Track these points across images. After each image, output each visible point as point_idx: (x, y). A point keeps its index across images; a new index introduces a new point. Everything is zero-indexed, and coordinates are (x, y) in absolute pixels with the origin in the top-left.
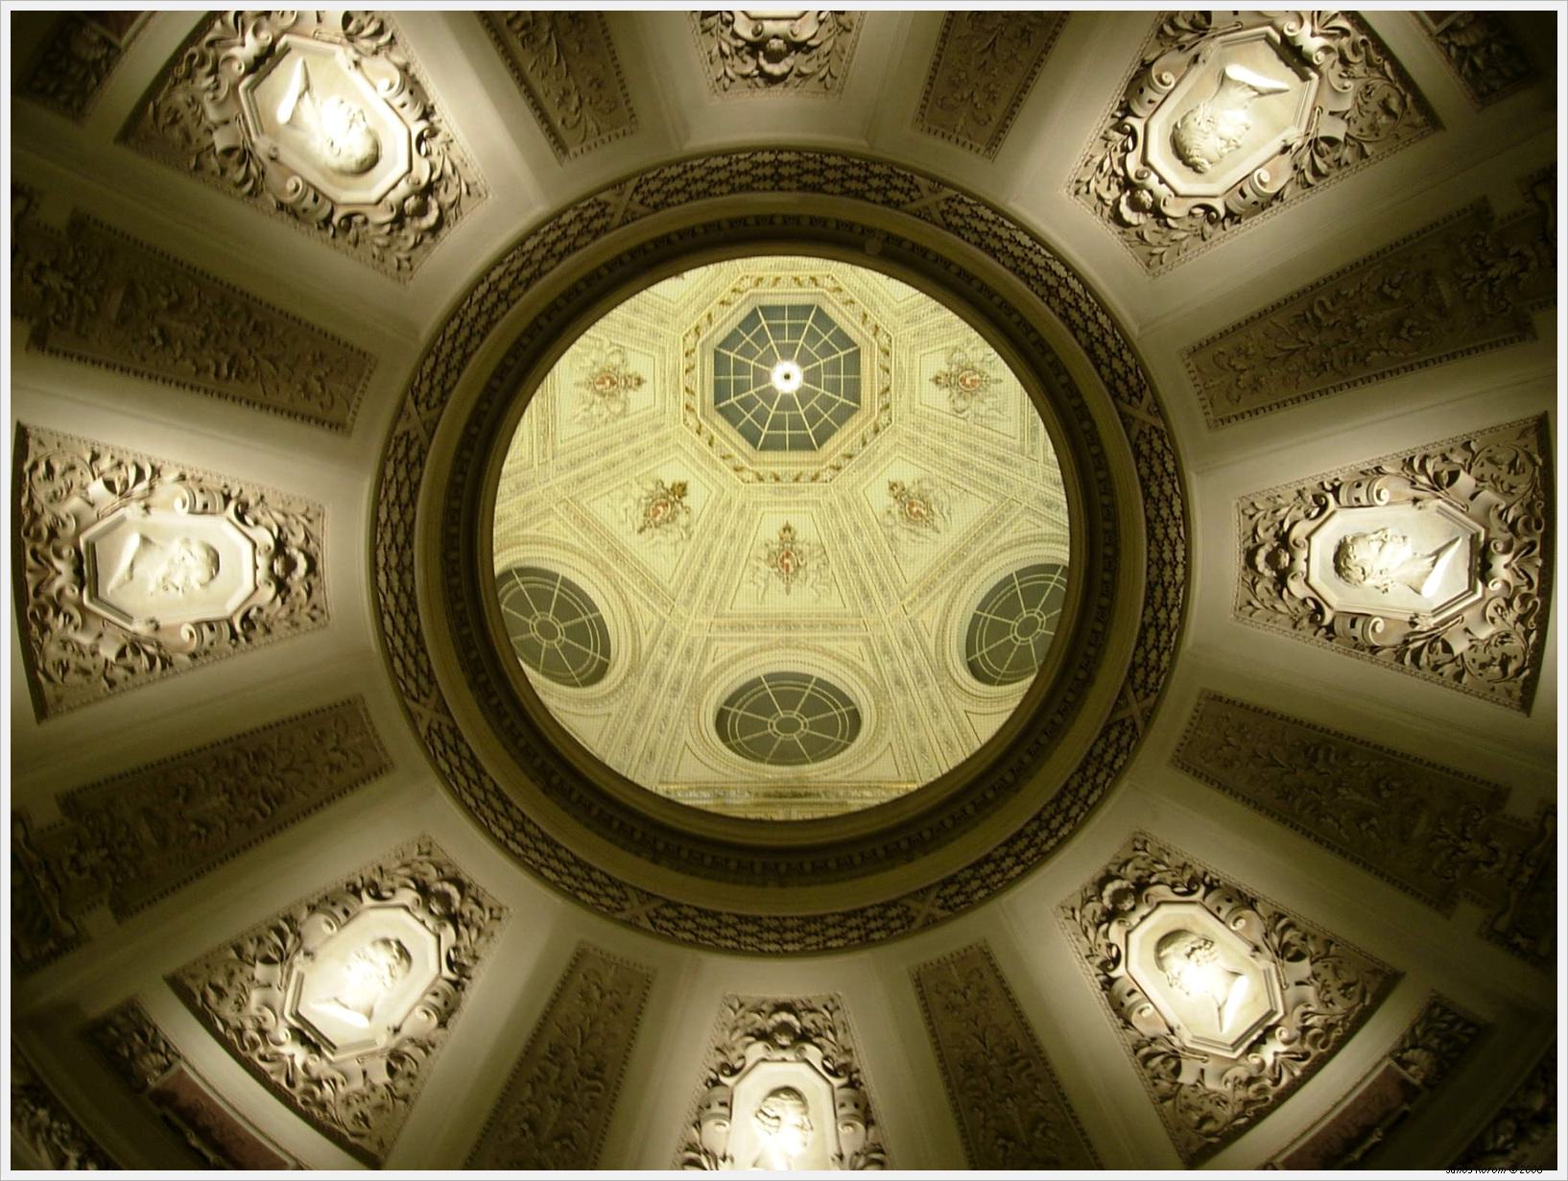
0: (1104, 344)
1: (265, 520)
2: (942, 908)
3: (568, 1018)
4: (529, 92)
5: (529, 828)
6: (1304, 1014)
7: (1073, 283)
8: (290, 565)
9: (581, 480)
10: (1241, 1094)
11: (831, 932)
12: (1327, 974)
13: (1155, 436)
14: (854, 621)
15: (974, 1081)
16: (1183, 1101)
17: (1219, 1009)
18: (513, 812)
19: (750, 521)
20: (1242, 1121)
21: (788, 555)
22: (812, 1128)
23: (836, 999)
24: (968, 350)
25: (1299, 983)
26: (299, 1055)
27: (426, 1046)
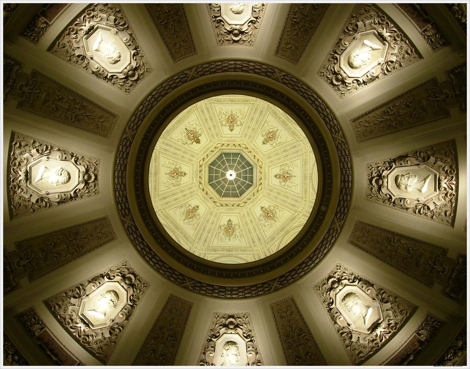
0: (295, 274)
1: (250, 29)
2: (128, 226)
3: (94, 112)
4: (370, 112)
5: (155, 102)
6: (93, 335)
7: (313, 265)
8: (236, 35)
9: (202, 111)
10: (68, 317)
11: (121, 192)
12: (105, 342)
13: (269, 288)
14: (157, 194)
15: (72, 235)
16: (65, 299)
17: (94, 310)
18: (161, 98)
20: (59, 317)
21: (177, 174)
22: (57, 185)
23: (99, 193)
24: (239, 230)
25: (102, 333)
26: (86, 28)
27: (86, 67)
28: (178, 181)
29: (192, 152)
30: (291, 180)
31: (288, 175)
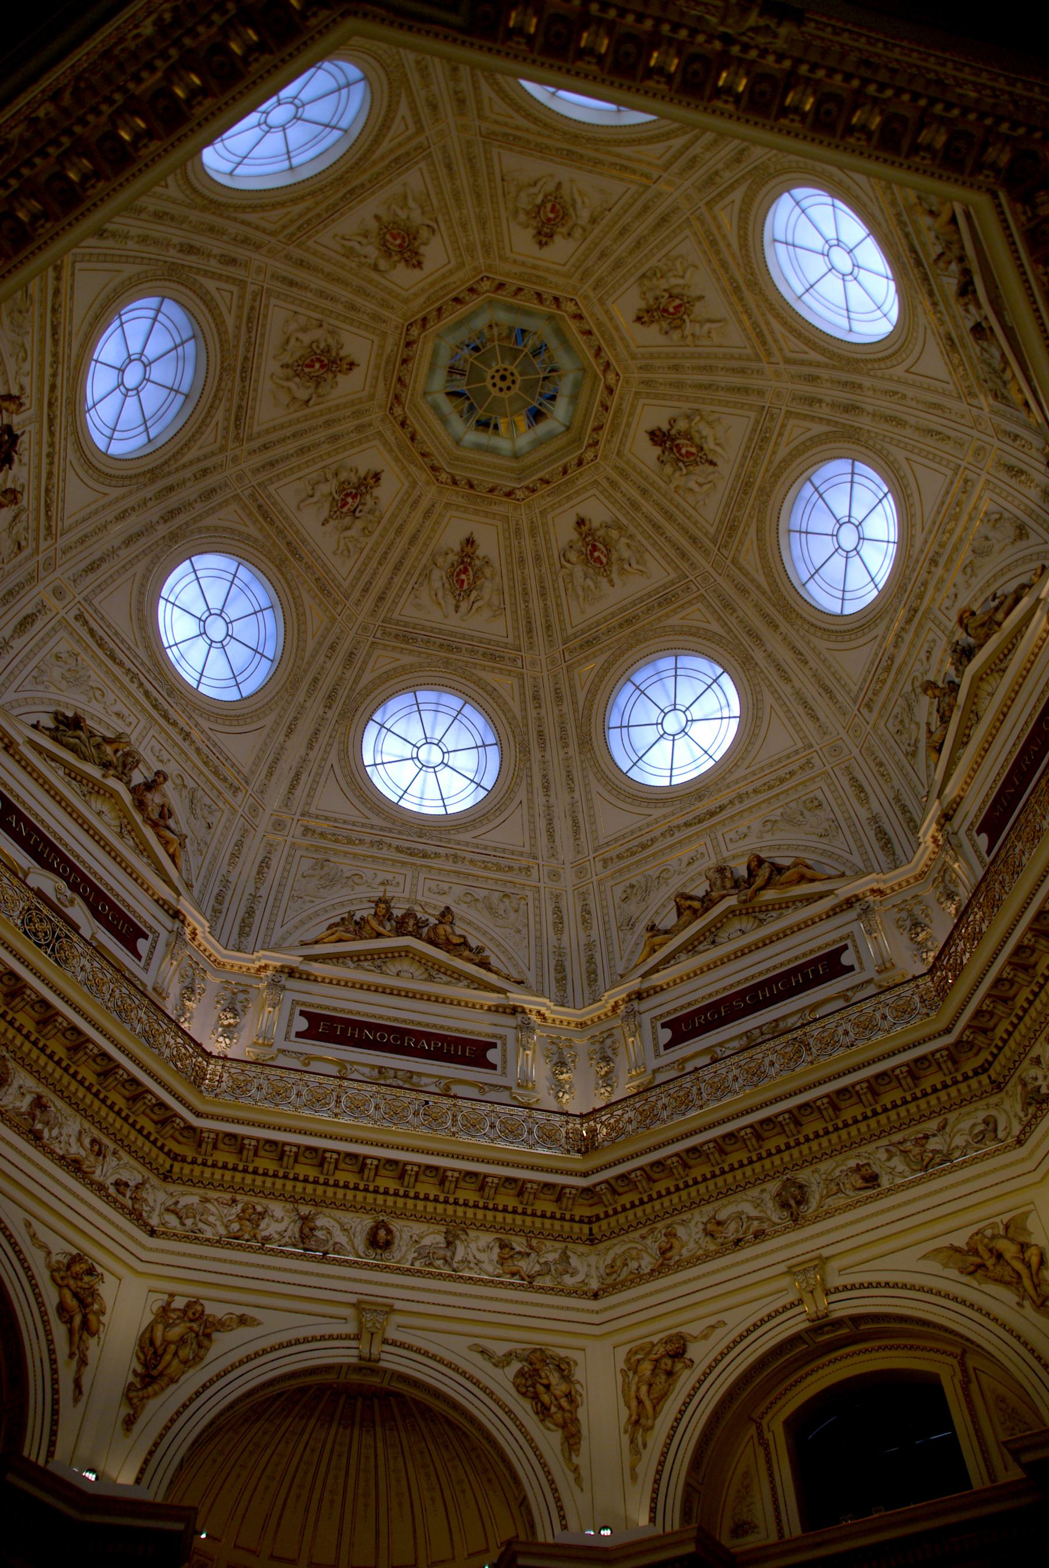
9: (694, 540)
19: (652, 356)
21: (665, 310)
28: (651, 289)
29: (657, 396)
30: (327, 505)
31: (345, 510)
